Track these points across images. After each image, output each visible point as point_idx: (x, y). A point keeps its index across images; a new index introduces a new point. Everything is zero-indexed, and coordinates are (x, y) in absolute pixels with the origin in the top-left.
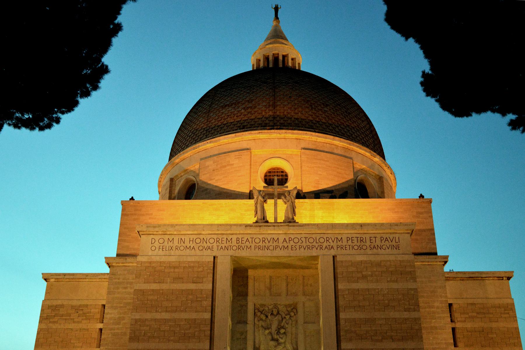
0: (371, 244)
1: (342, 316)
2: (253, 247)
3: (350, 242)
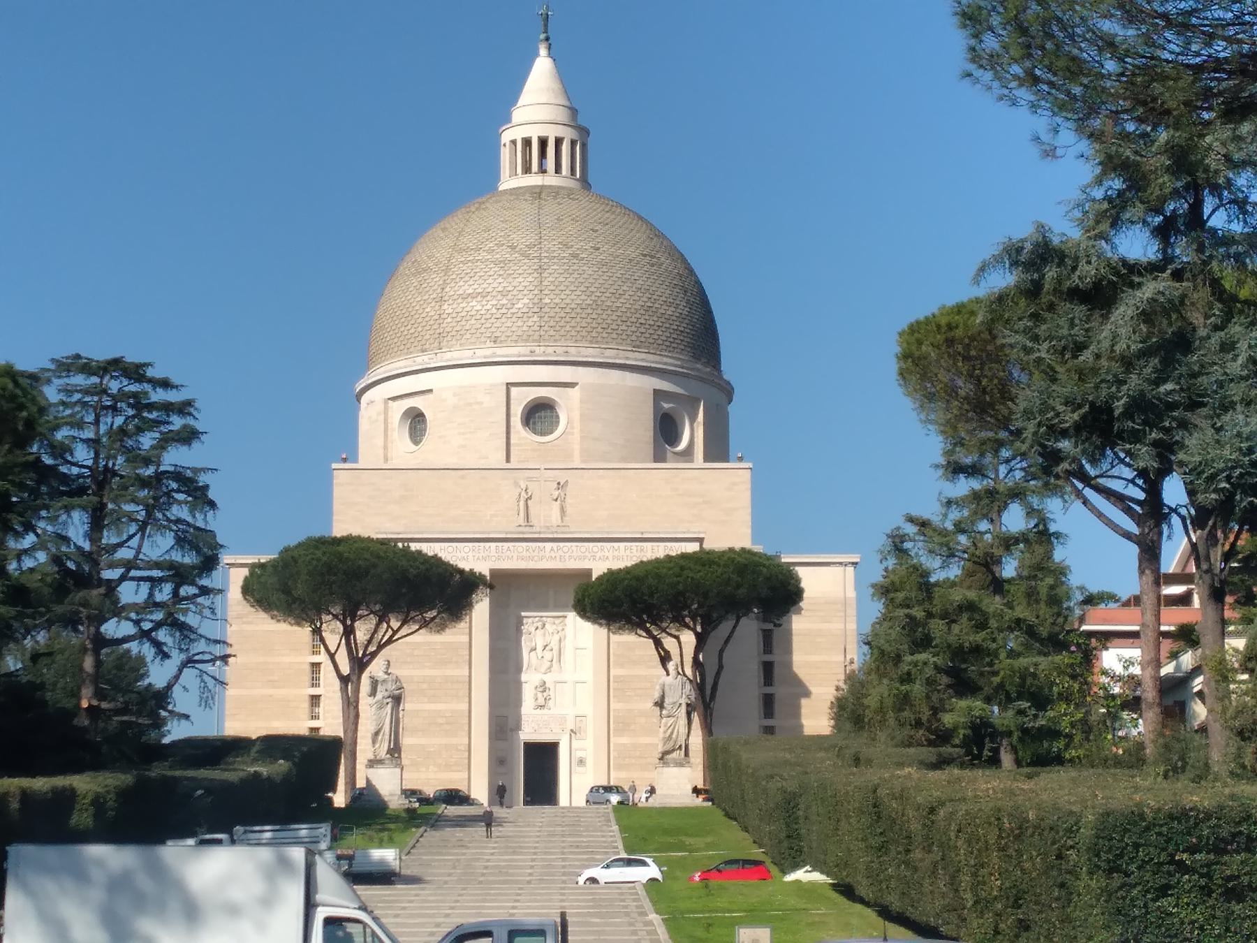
2: (515, 557)
3: (628, 551)
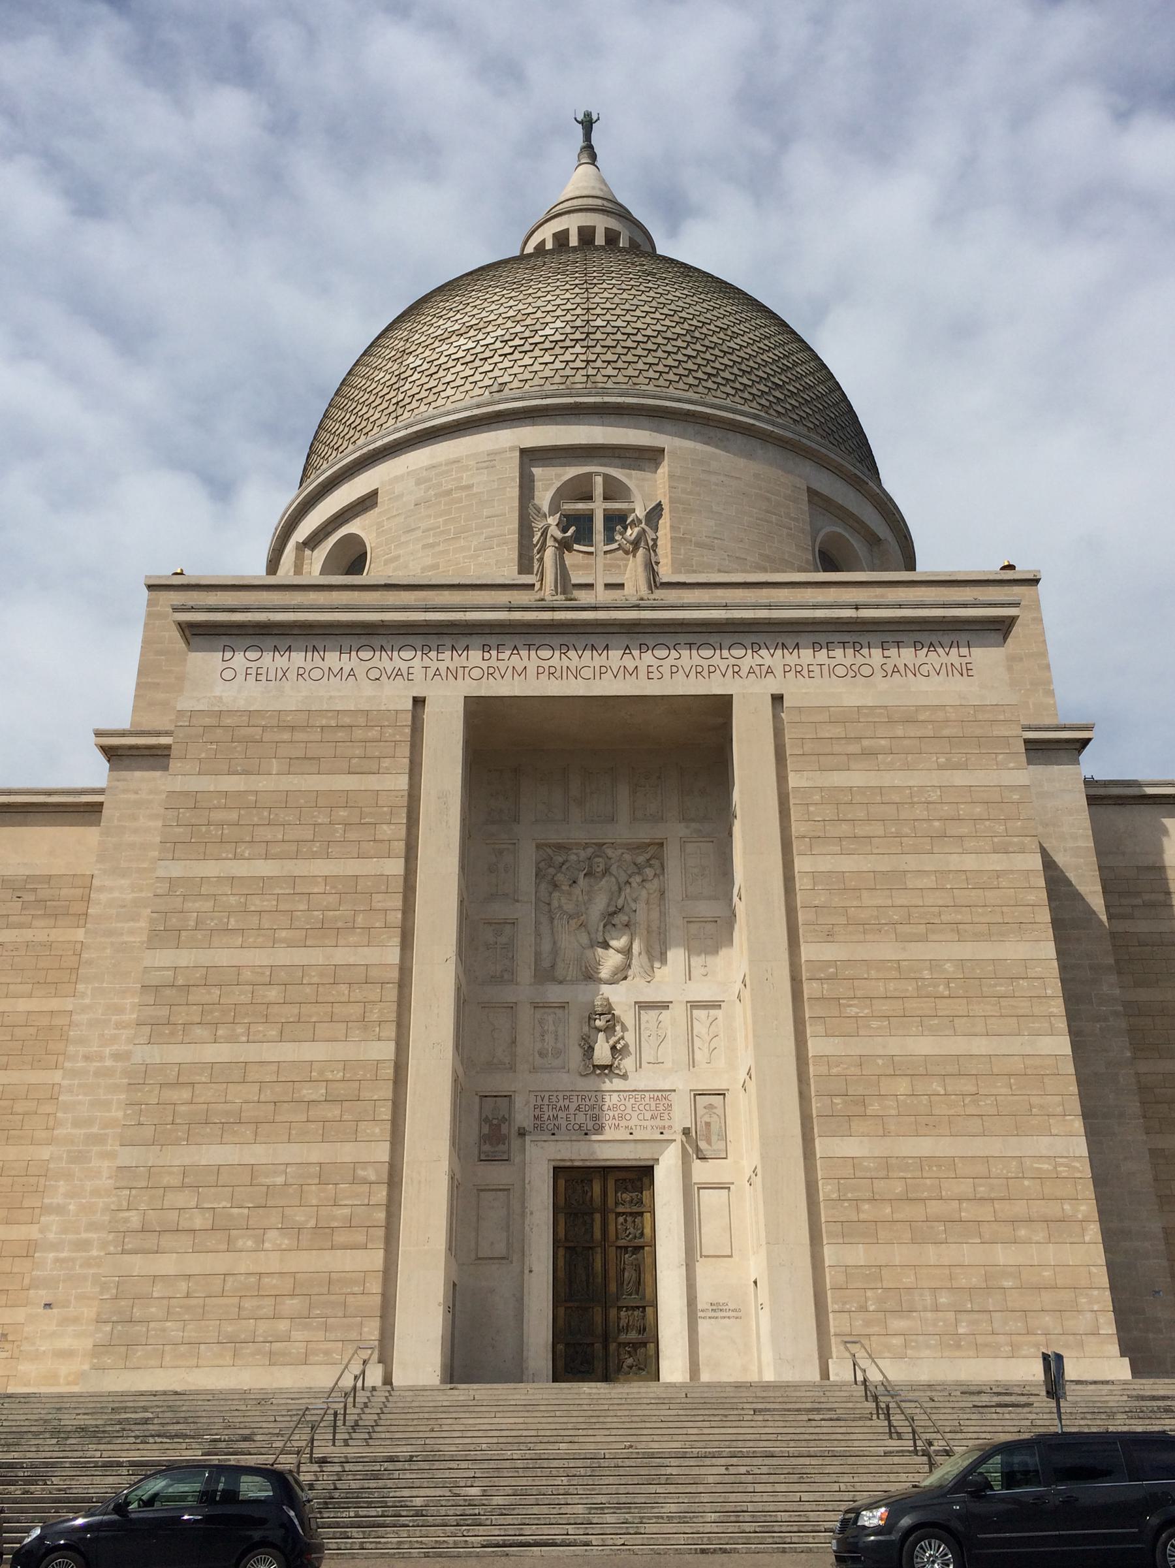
0: (885, 660)
1: (801, 864)
2: (532, 671)
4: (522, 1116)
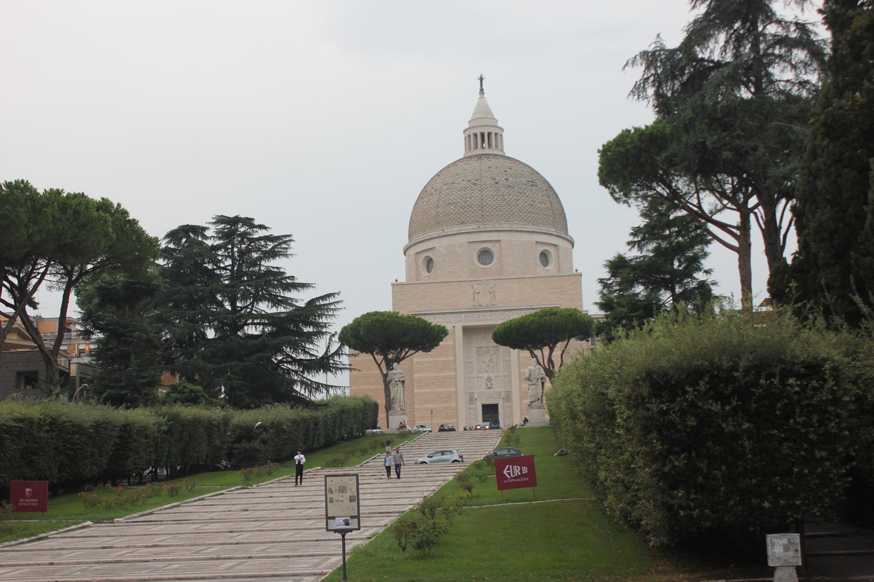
4: (476, 397)
